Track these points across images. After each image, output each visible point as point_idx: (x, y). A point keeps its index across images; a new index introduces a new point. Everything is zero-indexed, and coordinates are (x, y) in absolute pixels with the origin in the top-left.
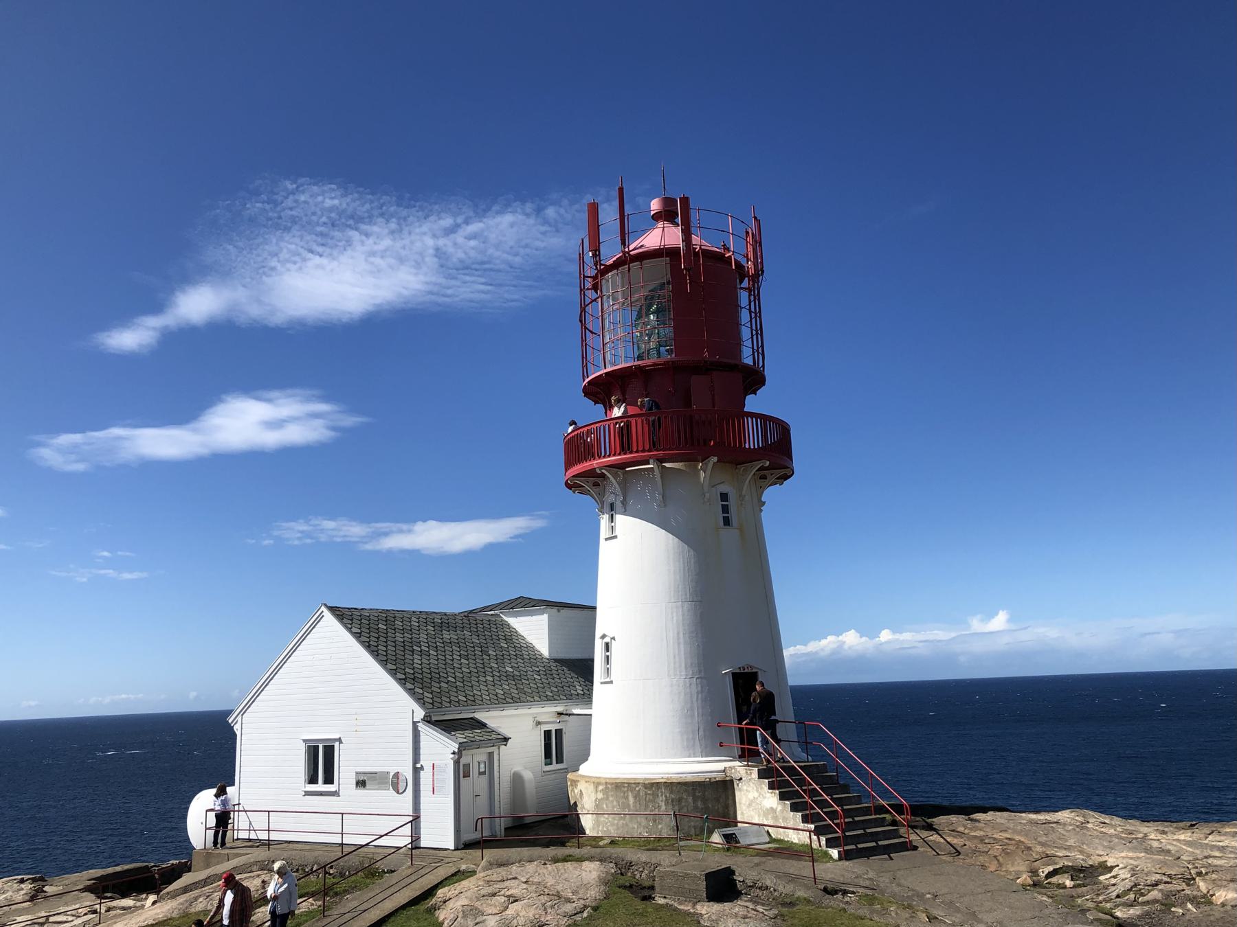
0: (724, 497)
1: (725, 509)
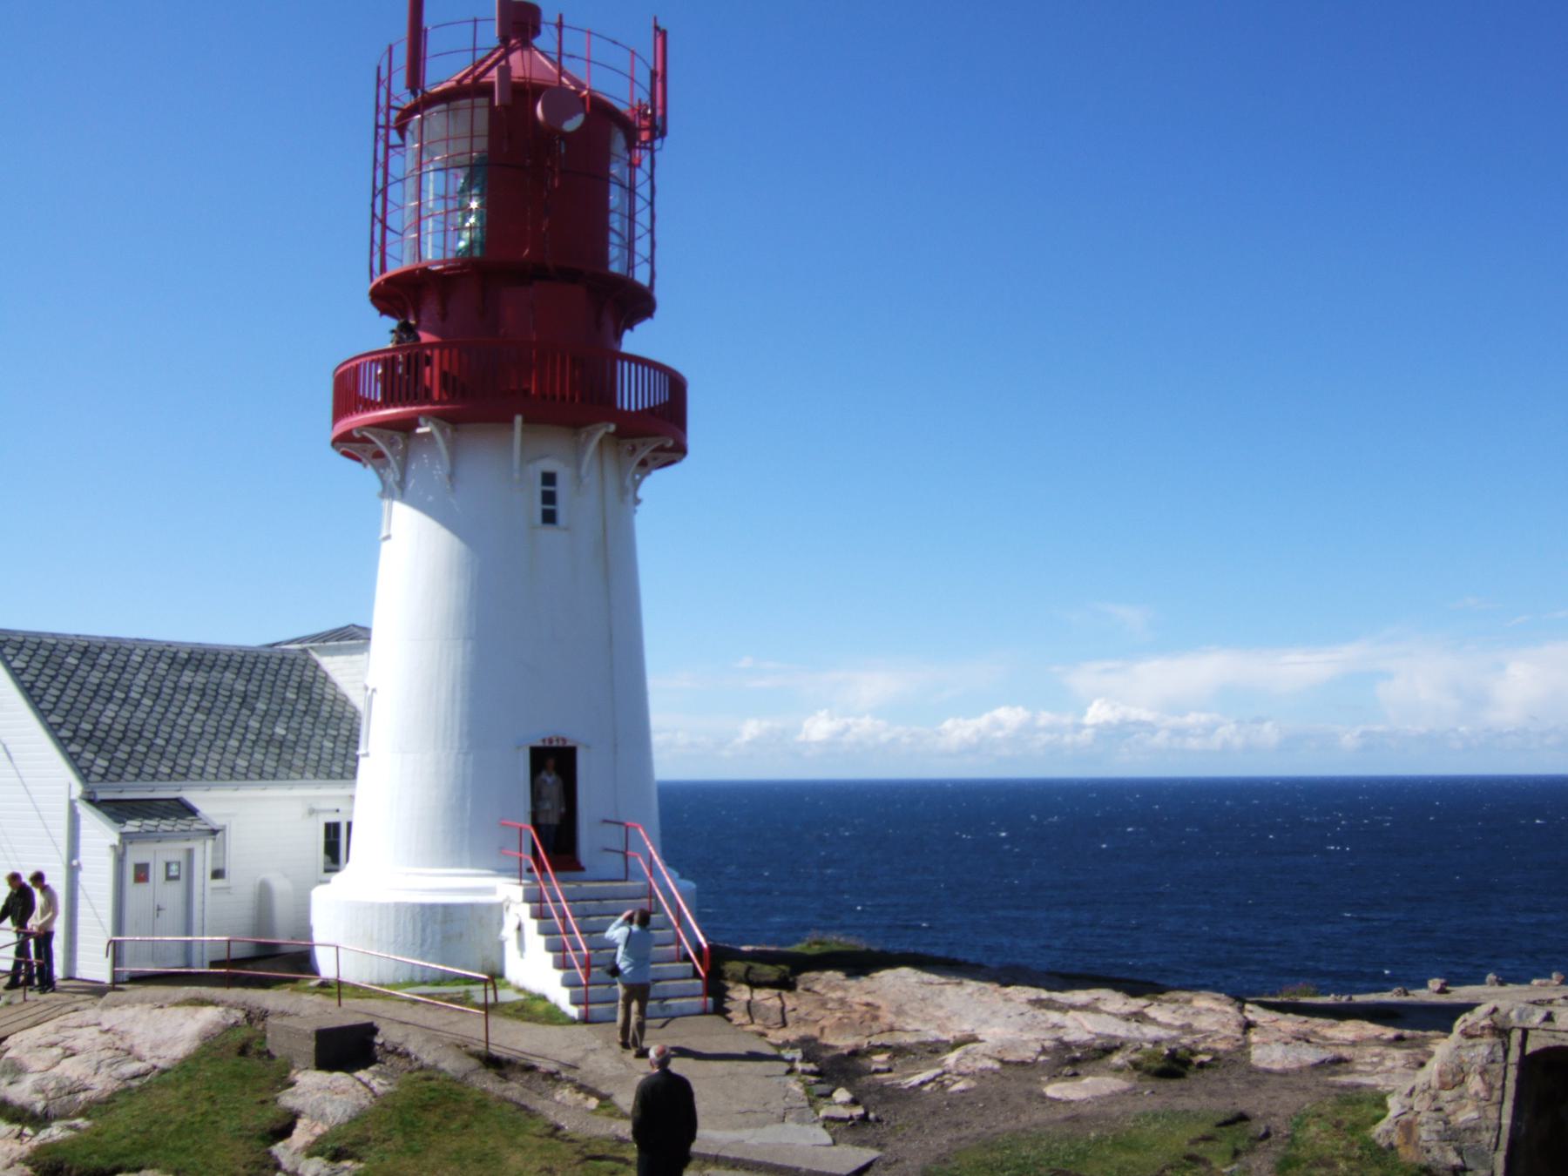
0: (549, 479)
1: (549, 498)
